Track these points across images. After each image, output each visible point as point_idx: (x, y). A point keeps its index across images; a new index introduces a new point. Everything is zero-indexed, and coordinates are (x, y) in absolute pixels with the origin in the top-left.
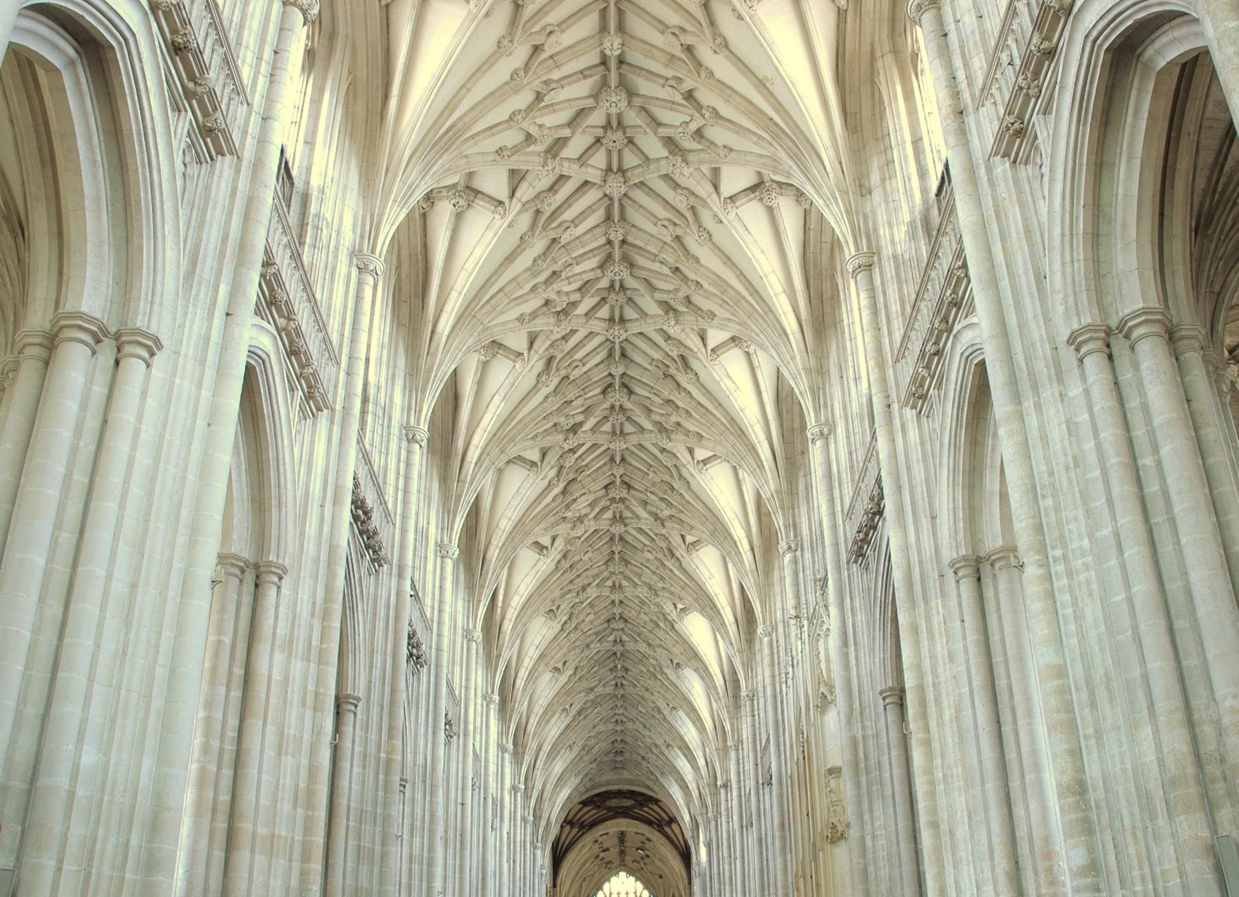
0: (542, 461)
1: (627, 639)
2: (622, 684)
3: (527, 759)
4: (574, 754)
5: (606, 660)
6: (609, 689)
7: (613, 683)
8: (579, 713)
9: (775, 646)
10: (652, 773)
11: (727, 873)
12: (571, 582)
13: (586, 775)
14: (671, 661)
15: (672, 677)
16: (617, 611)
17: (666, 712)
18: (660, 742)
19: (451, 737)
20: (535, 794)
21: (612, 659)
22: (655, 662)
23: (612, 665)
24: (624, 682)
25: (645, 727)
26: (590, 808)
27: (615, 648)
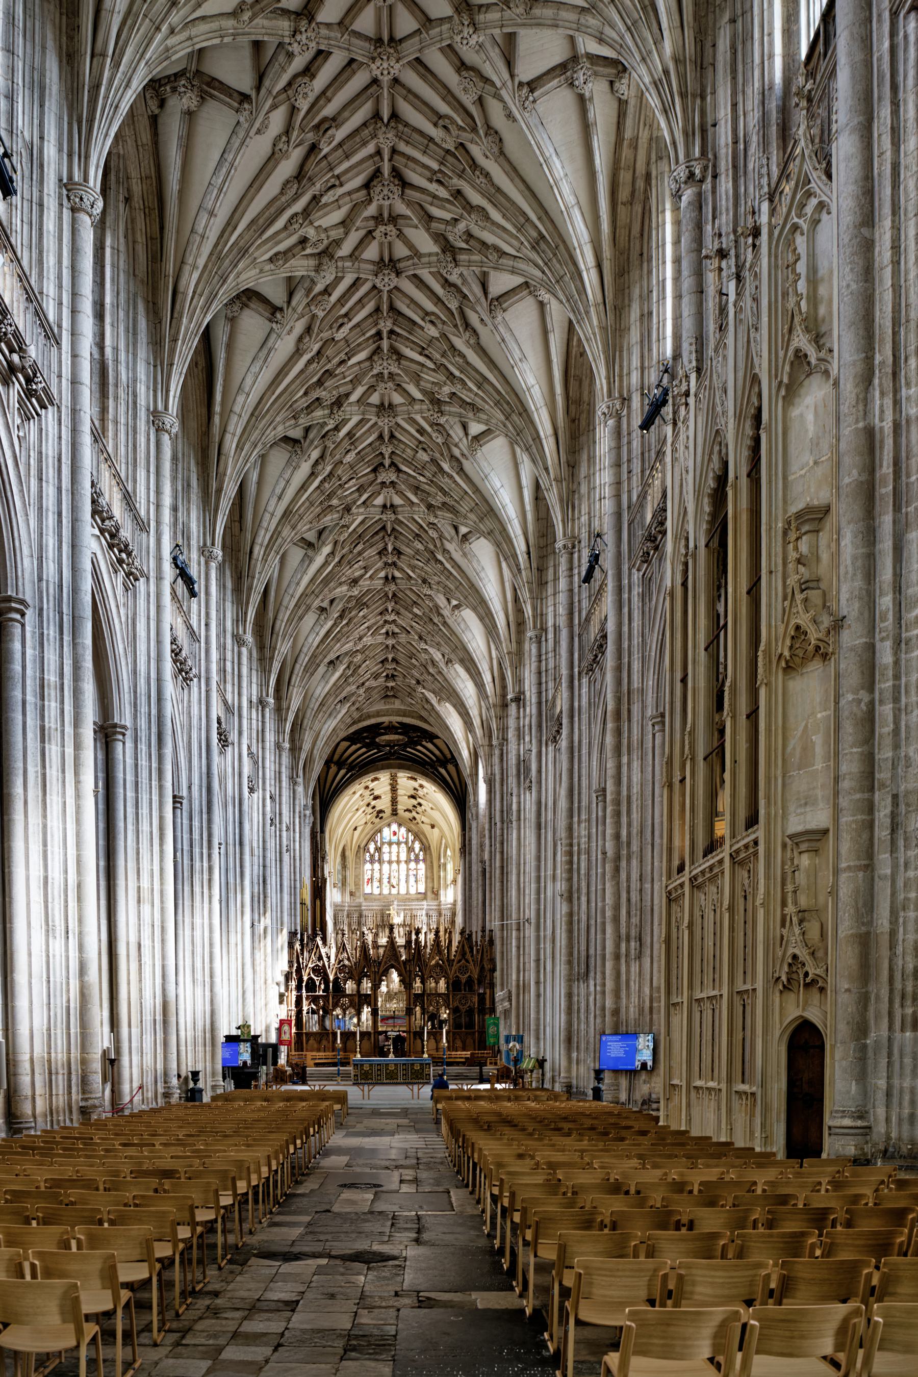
0: (258, 88)
2: (394, 578)
5: (372, 536)
6: (378, 583)
7: (382, 574)
9: (625, 432)
10: (427, 701)
12: (320, 383)
14: (456, 529)
15: (457, 556)
16: (387, 451)
17: (446, 612)
18: (437, 656)
20: (291, 717)
21: (381, 535)
22: (434, 535)
23: (381, 546)
24: (397, 574)
27: (384, 517)
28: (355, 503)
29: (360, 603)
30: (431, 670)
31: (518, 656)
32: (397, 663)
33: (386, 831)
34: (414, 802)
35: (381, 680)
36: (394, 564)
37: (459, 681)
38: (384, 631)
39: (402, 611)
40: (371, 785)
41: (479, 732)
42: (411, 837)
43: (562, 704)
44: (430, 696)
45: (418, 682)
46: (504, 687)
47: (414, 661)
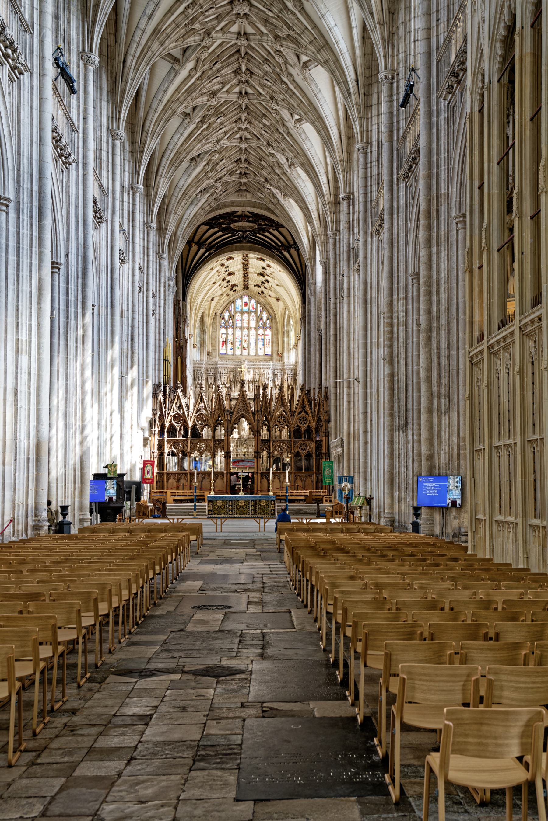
1: (253, 32)
2: (246, 93)
3: (146, 159)
4: (198, 169)
5: (229, 58)
6: (234, 97)
7: (237, 89)
8: (202, 122)
10: (274, 196)
11: (346, 286)
13: (212, 194)
19: (21, 73)
21: (236, 57)
23: (236, 66)
24: (249, 90)
25: (269, 144)
26: (216, 229)
28: (214, 28)
29: (218, 112)
30: (277, 171)
31: (349, 162)
32: (249, 163)
33: (239, 303)
34: (262, 279)
35: (236, 176)
36: (247, 82)
37: (300, 181)
38: (238, 136)
39: (253, 121)
40: (227, 263)
41: (316, 223)
42: (260, 308)
43: (383, 204)
44: (276, 192)
45: (266, 180)
46: (337, 188)
47: (263, 162)
